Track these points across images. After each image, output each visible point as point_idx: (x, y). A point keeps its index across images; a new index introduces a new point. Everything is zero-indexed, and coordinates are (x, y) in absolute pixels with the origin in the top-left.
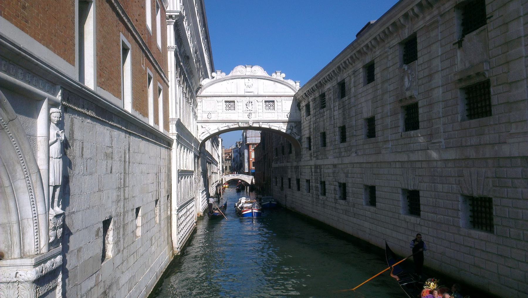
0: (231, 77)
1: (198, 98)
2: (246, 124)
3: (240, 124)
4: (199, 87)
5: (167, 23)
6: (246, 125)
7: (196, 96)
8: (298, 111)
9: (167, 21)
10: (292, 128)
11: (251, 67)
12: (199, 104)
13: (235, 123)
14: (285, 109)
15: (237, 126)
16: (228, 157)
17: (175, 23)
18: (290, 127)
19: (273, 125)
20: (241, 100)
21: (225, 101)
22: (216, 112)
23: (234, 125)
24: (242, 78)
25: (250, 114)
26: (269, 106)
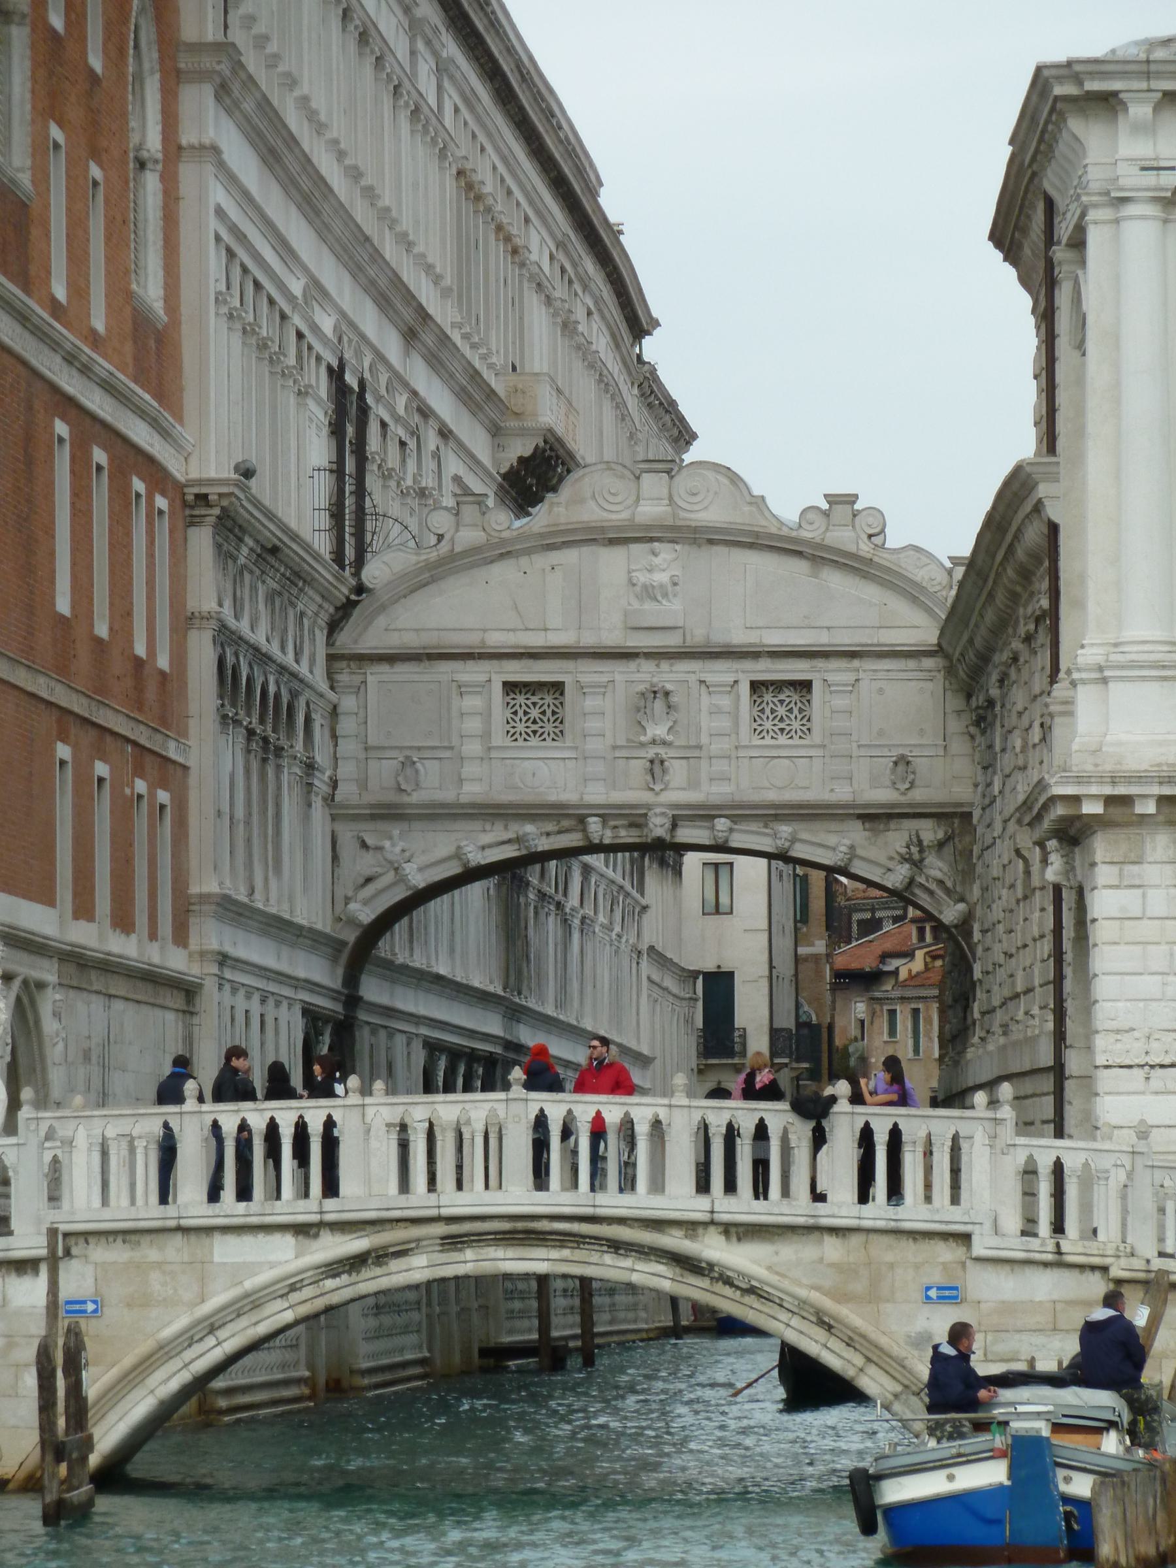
0: (542, 535)
1: (344, 664)
2: (632, 825)
3: (594, 824)
4: (348, 598)
5: (188, 519)
6: (634, 832)
7: (331, 658)
8: (959, 746)
9: (188, 512)
10: (916, 857)
11: (668, 472)
12: (348, 703)
13: (566, 823)
14: (881, 733)
15: (572, 840)
16: (918, 964)
17: (218, 517)
18: (908, 847)
19: (804, 836)
20: (604, 679)
21: (505, 684)
22: (447, 754)
23: (560, 832)
24: (613, 542)
25: (657, 762)
26: (781, 711)
